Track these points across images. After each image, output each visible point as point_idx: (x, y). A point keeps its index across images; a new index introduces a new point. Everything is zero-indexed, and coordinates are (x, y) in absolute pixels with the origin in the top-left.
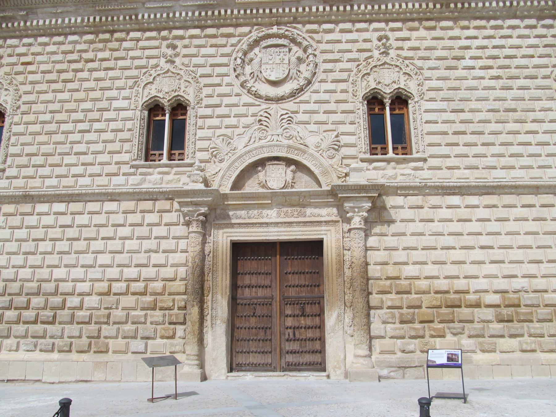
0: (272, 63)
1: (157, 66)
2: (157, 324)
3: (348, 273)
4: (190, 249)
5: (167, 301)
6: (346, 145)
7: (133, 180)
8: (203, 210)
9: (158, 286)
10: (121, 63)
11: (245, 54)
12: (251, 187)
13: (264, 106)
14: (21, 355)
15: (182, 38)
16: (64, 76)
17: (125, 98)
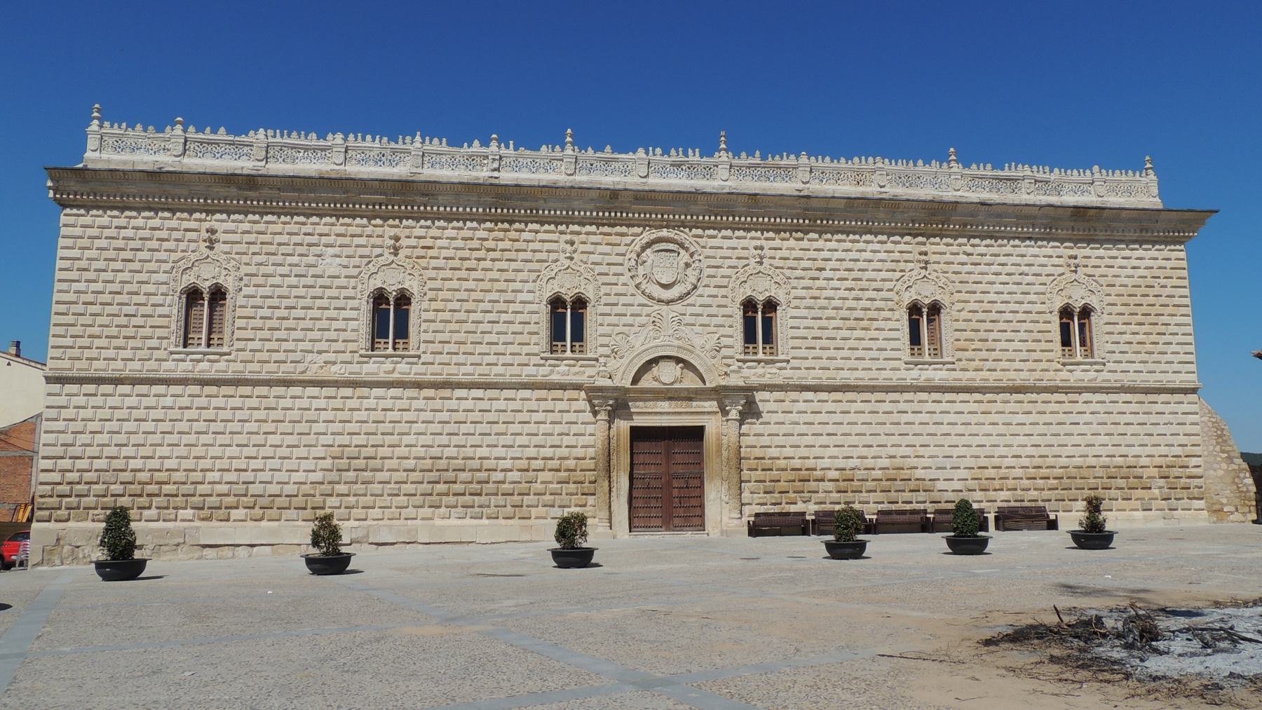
0: (663, 267)
1: (557, 261)
2: (572, 494)
3: (725, 454)
4: (597, 433)
5: (579, 475)
6: (725, 347)
7: (542, 371)
8: (611, 402)
9: (571, 463)
10: (522, 255)
11: (638, 256)
12: (646, 382)
13: (656, 307)
14: (453, 522)
15: (579, 233)
16: (467, 264)
17: (529, 292)
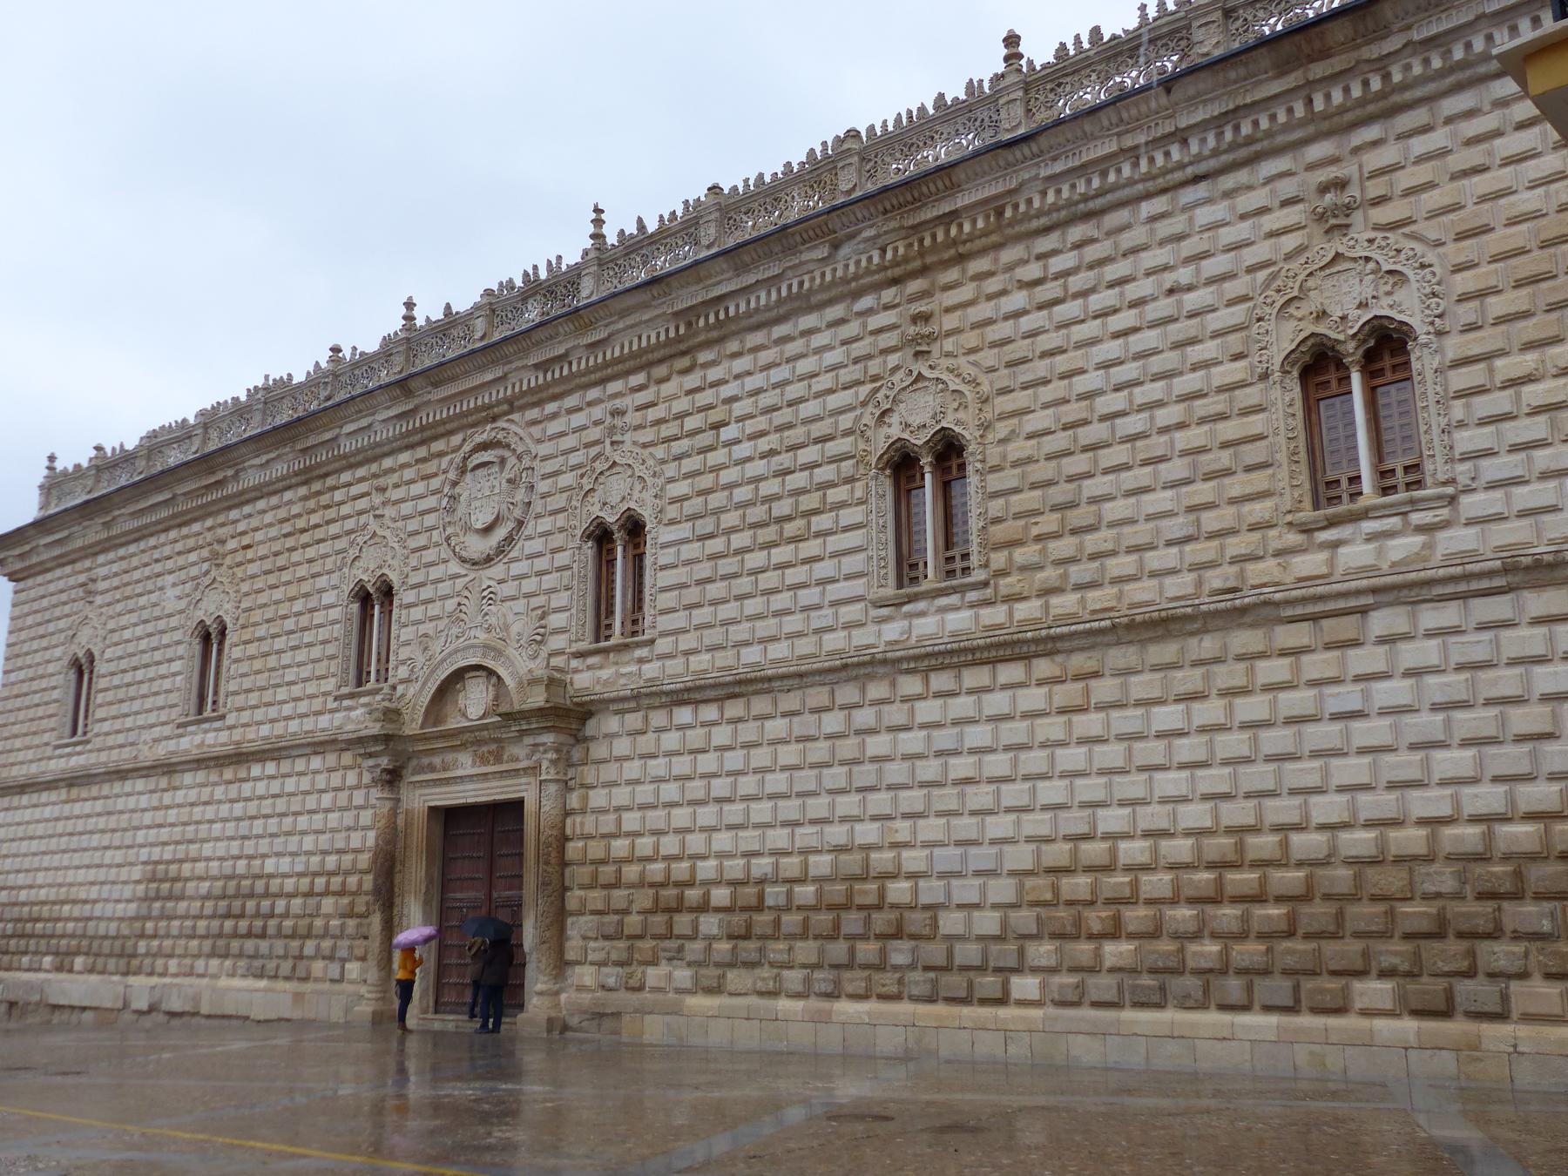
0: (483, 498)
